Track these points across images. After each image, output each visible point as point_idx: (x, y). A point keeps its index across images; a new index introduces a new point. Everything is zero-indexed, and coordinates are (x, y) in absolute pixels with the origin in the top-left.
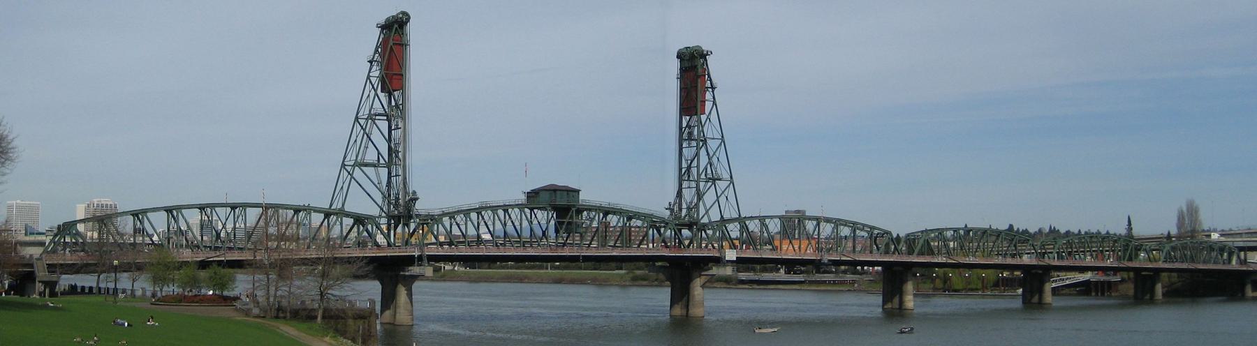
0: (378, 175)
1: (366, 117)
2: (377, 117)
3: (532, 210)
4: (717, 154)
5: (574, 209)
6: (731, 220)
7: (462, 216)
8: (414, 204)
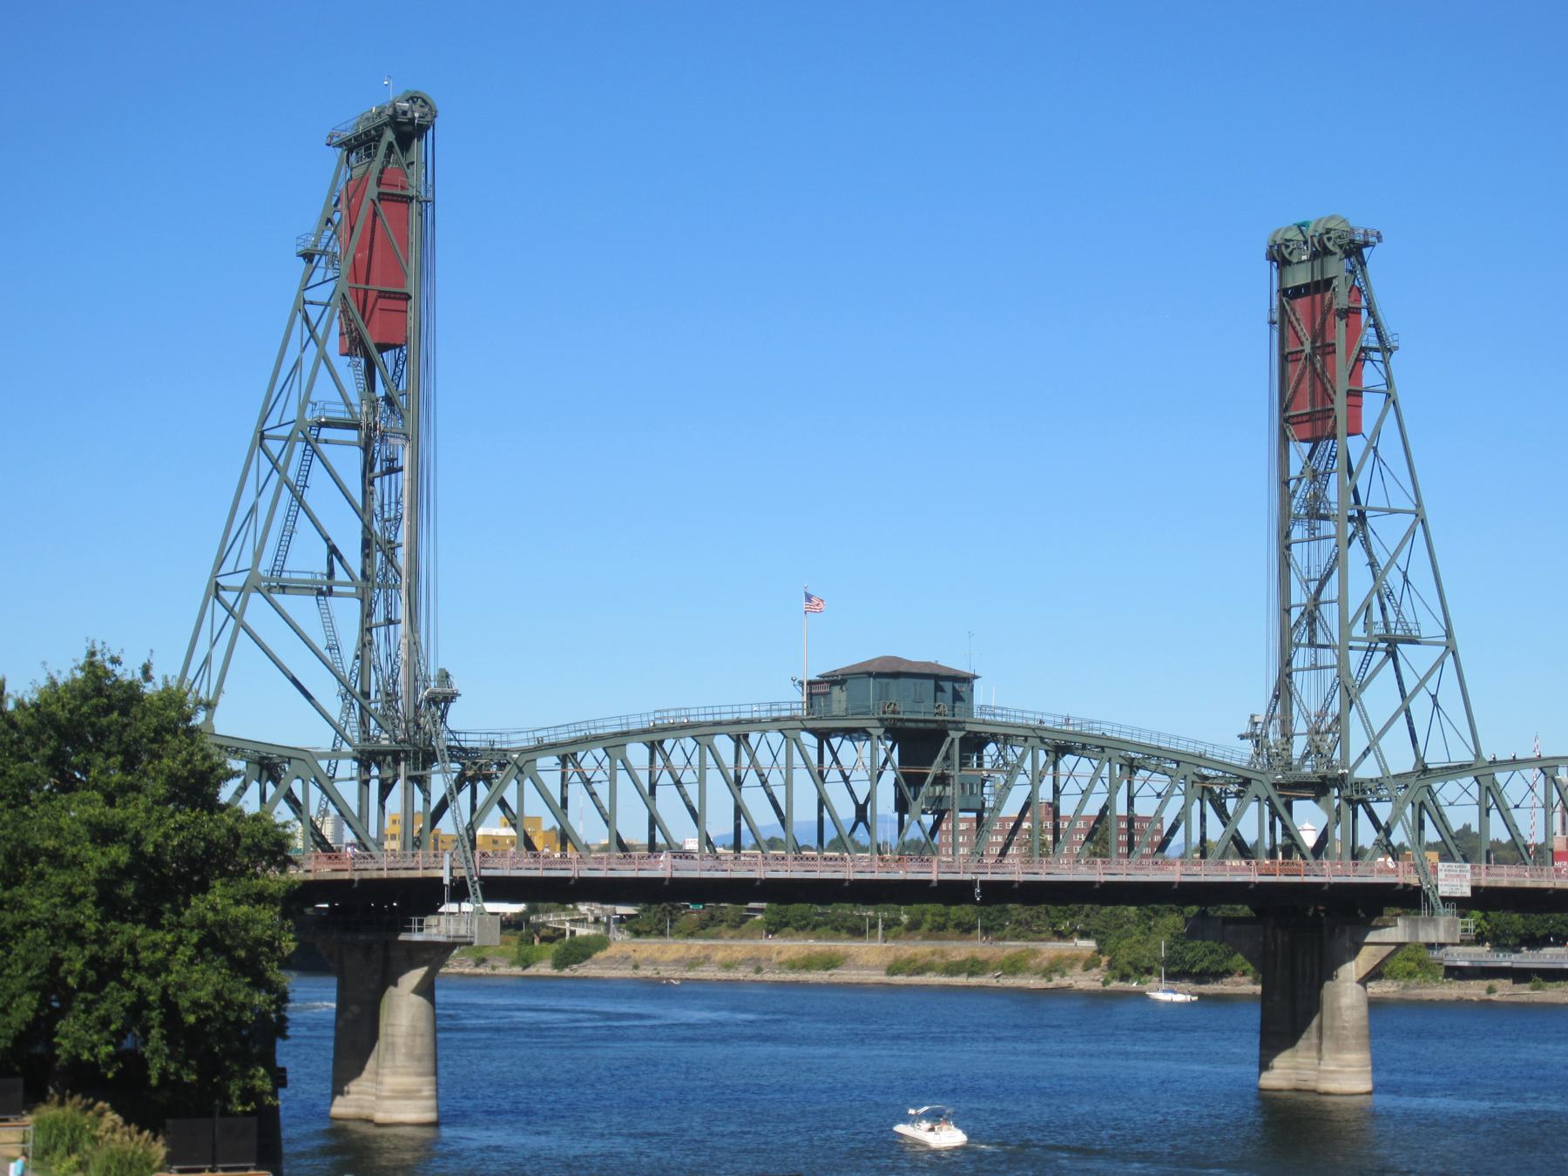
0: (328, 622)
1: (286, 431)
2: (326, 433)
3: (823, 736)
4: (1401, 560)
5: (956, 735)
6: (1453, 771)
7: (600, 753)
8: (443, 716)
